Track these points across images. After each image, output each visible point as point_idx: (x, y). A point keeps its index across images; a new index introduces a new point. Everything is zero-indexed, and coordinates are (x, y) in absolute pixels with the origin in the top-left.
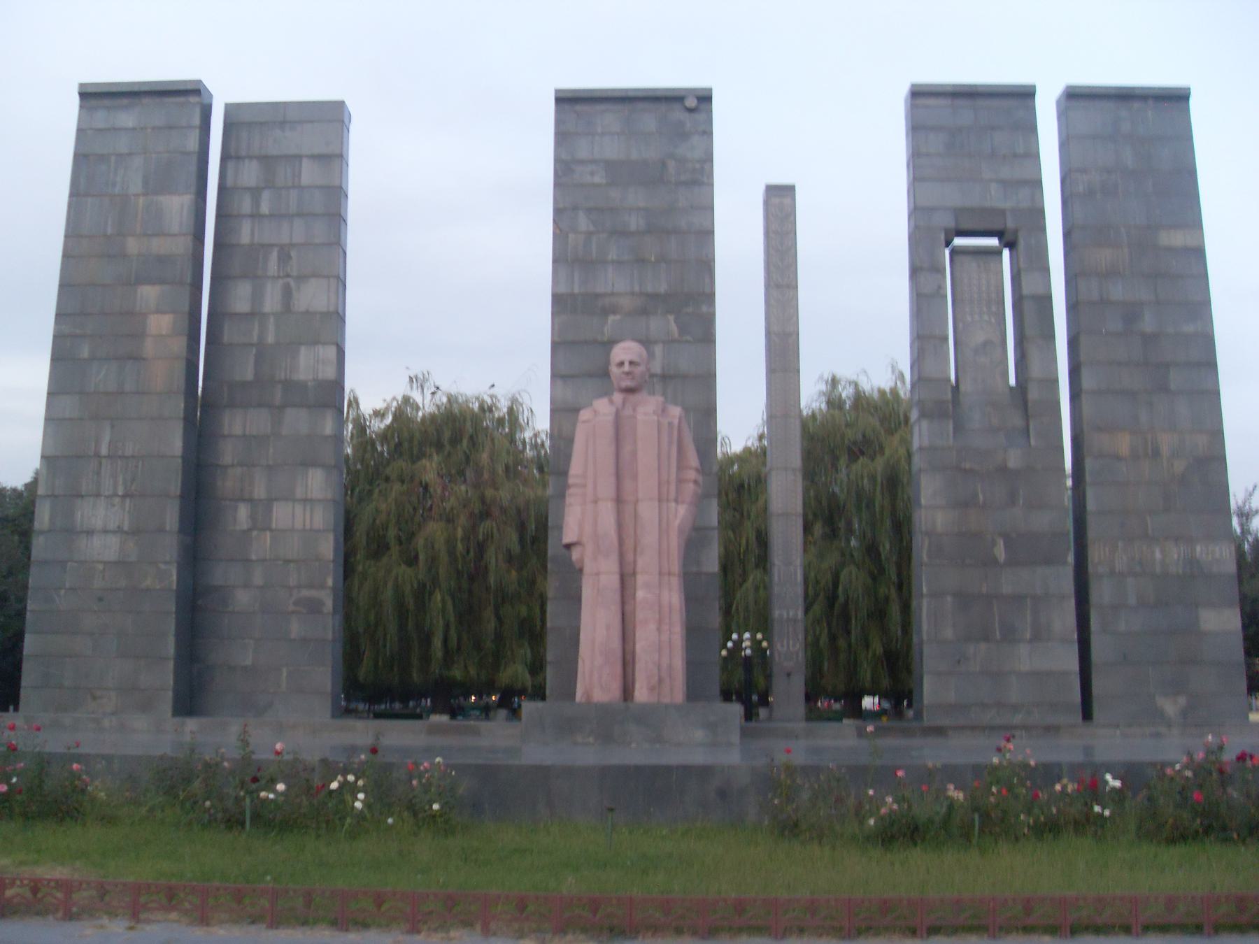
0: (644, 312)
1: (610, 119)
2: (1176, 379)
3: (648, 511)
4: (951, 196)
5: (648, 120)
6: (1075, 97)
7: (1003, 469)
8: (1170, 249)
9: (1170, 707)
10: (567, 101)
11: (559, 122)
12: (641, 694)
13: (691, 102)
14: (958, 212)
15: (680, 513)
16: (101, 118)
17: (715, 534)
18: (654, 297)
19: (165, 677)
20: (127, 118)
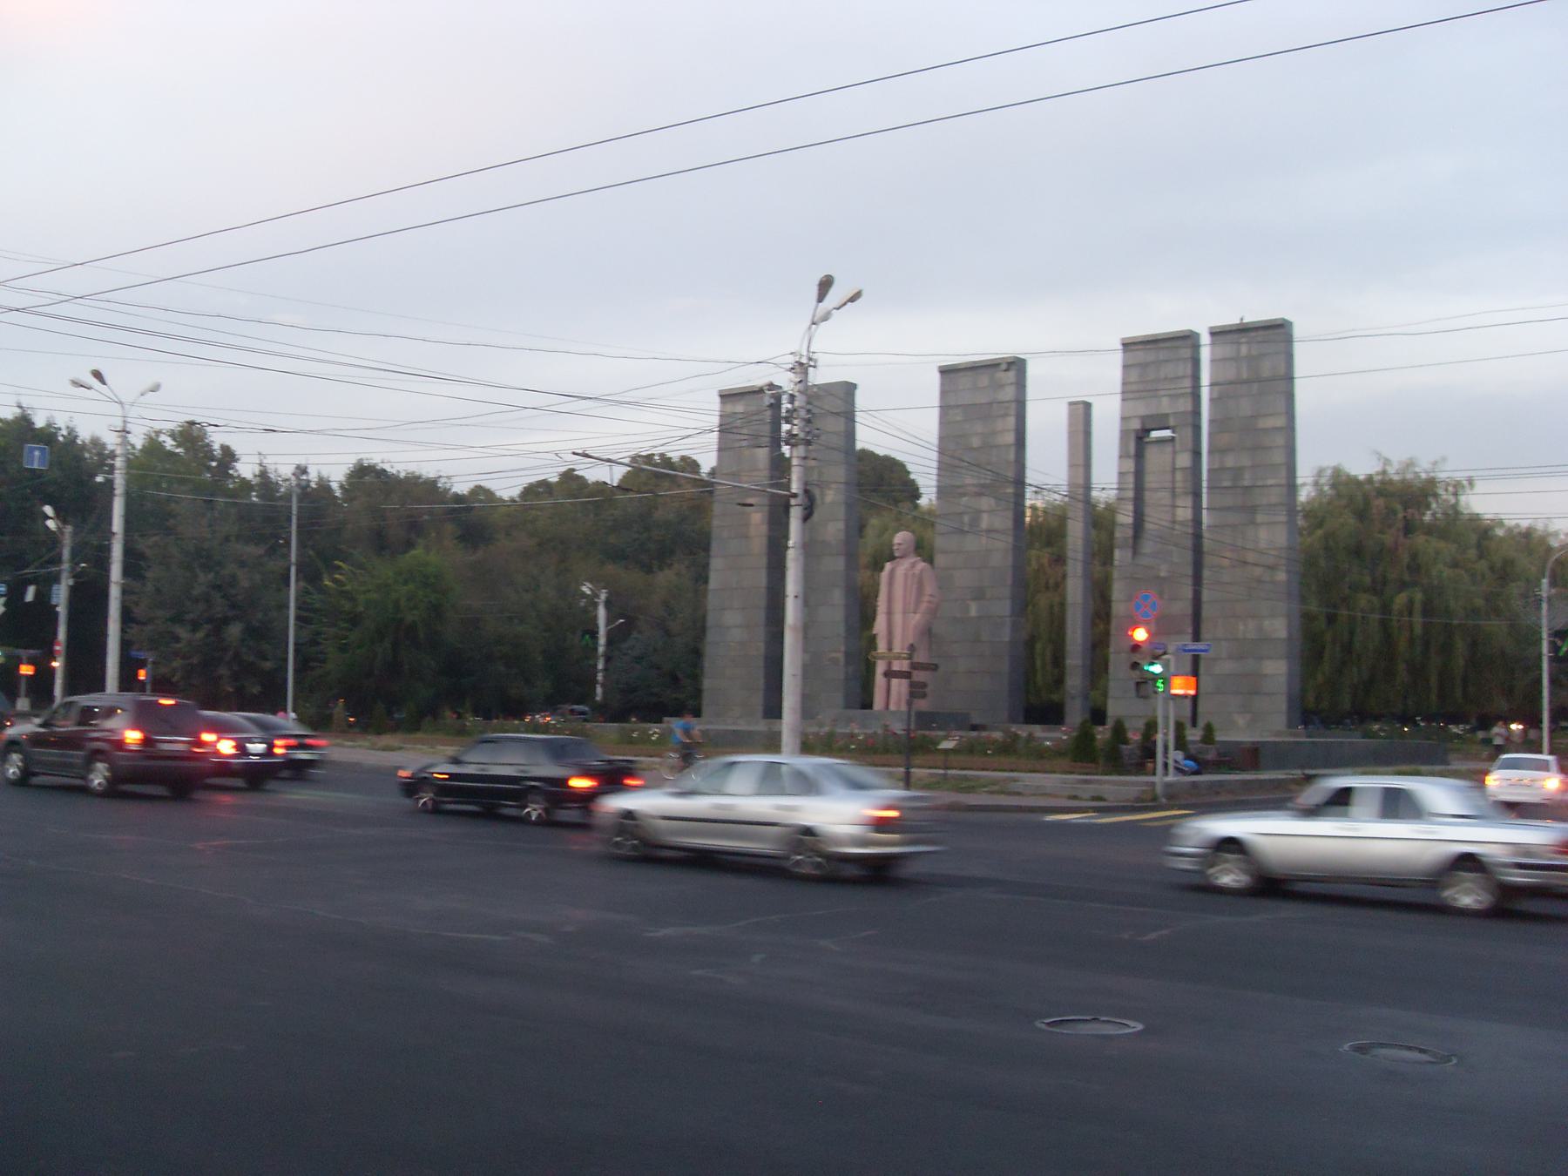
0: (980, 494)
1: (964, 381)
2: (1260, 518)
3: (898, 618)
4: (1142, 409)
5: (984, 380)
6: (1216, 333)
7: (1158, 577)
8: (1265, 430)
9: (1241, 721)
10: (946, 372)
11: (942, 385)
12: (892, 707)
13: (1004, 367)
14: (1143, 418)
15: (916, 619)
16: (729, 408)
17: (1008, 620)
18: (983, 486)
19: (758, 700)
20: (739, 408)
